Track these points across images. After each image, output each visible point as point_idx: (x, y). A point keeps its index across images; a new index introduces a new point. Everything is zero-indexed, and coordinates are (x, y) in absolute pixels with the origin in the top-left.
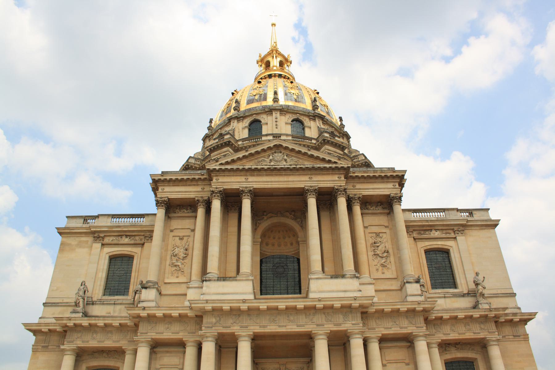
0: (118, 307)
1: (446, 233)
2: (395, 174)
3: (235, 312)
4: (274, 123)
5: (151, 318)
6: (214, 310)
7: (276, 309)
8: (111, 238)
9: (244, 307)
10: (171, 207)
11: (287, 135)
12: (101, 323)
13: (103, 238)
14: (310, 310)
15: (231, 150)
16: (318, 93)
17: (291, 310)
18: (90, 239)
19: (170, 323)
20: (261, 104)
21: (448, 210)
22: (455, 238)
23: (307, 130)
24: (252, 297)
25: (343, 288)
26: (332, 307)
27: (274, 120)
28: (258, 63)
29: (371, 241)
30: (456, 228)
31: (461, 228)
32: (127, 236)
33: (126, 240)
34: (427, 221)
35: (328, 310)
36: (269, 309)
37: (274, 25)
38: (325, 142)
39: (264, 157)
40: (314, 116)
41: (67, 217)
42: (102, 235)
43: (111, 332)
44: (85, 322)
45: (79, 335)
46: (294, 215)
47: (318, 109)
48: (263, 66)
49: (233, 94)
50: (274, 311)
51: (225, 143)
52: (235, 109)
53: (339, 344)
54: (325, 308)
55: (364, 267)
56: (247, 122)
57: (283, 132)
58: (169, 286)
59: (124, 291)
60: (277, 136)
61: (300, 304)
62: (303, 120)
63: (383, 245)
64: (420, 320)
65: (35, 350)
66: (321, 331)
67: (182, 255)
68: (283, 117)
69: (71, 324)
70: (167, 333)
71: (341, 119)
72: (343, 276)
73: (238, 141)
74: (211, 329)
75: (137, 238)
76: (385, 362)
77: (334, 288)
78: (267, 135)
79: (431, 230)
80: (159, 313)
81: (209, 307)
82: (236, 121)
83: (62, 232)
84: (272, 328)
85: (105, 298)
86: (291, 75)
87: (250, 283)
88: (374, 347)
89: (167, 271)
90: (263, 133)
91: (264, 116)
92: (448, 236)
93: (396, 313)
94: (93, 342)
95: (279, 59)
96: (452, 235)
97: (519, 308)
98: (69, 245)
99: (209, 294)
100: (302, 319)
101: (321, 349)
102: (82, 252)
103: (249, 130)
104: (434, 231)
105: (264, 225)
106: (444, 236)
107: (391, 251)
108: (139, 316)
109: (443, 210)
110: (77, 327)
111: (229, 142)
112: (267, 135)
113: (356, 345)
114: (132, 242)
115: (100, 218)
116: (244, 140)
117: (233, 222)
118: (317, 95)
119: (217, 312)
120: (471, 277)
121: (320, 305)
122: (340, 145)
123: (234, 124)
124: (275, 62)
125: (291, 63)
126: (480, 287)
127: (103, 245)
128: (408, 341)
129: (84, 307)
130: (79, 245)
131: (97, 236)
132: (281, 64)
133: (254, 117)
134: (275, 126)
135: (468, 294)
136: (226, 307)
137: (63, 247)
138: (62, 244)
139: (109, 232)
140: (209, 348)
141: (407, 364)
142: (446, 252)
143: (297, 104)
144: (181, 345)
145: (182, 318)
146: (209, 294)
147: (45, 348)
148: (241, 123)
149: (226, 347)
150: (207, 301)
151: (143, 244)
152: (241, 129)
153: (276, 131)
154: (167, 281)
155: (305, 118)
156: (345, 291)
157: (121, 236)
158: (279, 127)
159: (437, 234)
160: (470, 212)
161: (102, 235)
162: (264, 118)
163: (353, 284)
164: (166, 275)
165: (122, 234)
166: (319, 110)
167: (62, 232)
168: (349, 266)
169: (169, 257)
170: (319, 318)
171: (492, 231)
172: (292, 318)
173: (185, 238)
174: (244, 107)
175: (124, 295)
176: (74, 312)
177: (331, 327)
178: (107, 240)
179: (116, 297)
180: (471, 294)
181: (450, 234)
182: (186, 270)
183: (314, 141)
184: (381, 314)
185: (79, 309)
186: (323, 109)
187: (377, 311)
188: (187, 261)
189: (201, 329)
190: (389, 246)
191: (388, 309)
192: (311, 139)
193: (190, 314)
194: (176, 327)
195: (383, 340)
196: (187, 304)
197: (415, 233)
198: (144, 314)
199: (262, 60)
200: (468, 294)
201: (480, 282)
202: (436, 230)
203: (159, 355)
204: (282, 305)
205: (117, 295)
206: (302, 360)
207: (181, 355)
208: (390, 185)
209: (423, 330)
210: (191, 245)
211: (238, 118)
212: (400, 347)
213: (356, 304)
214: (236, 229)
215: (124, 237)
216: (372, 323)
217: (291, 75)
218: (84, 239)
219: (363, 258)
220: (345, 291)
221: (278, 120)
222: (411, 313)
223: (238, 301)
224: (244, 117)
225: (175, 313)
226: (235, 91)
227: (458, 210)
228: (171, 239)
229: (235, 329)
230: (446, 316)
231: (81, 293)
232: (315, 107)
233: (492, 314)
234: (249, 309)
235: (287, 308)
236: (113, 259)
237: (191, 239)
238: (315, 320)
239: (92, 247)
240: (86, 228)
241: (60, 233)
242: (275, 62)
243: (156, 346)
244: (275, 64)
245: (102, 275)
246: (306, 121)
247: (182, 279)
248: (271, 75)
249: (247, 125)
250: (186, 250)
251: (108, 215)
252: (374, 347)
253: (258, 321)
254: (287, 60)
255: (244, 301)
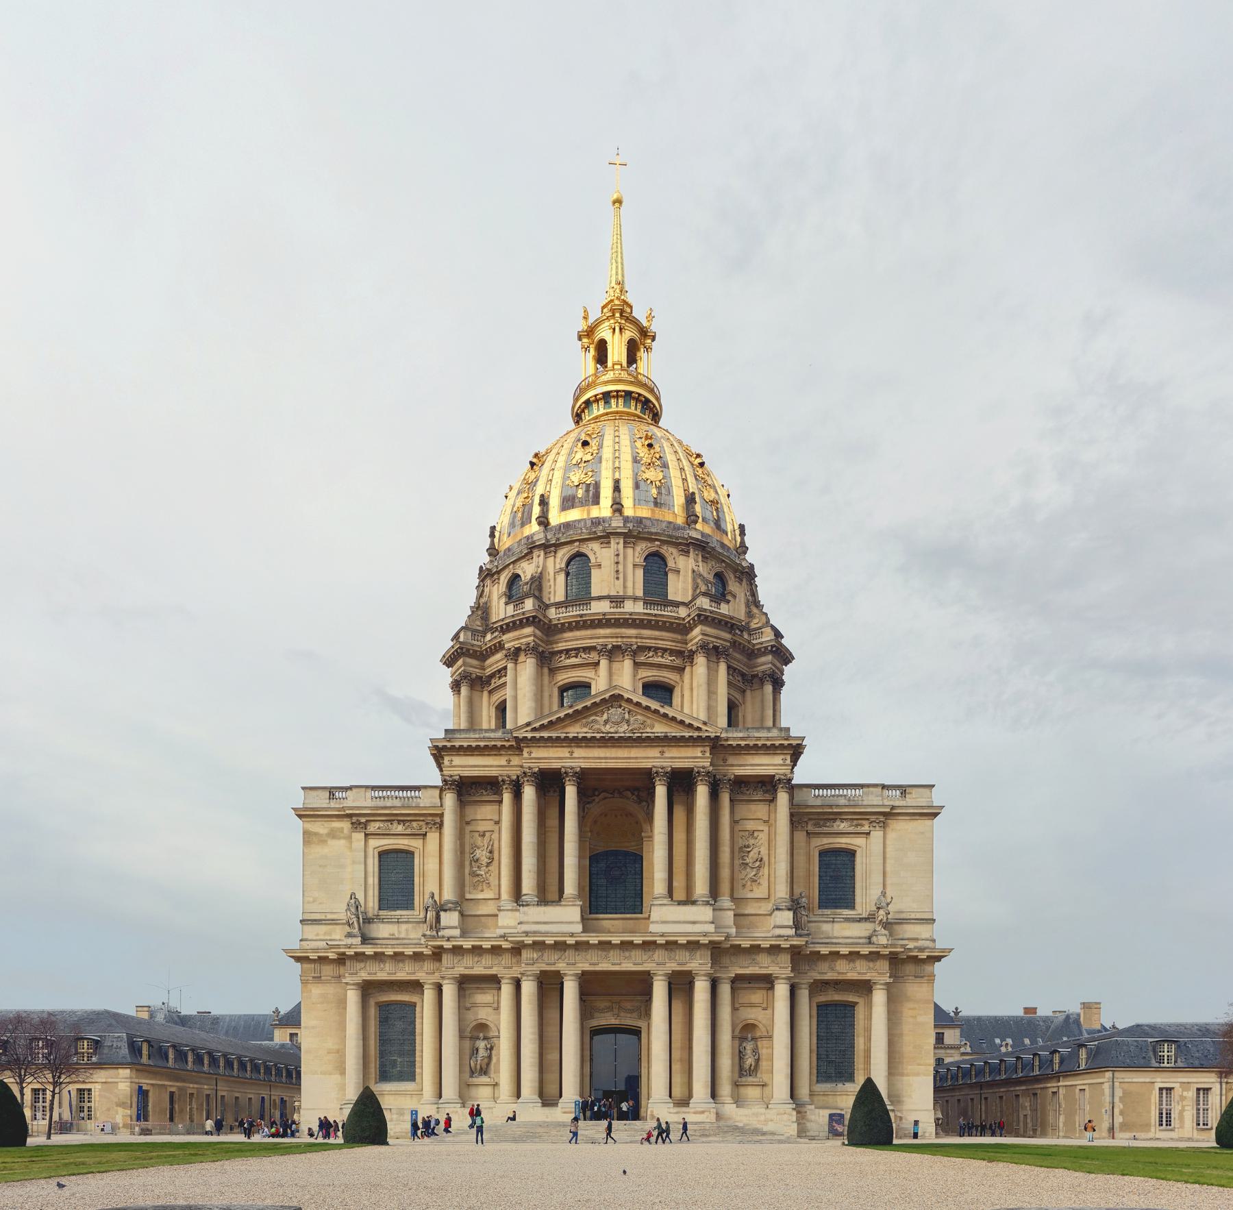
0: (404, 927)
1: (857, 825)
2: (786, 743)
3: (560, 946)
4: (613, 567)
5: (457, 950)
6: (535, 943)
7: (609, 943)
8: (377, 825)
9: (571, 941)
10: (468, 790)
11: (635, 599)
12: (389, 951)
13: (366, 825)
14: (648, 946)
15: (538, 632)
16: (702, 465)
17: (626, 946)
18: (345, 825)
19: (480, 955)
20: (589, 513)
21: (868, 786)
22: (868, 834)
23: (670, 576)
24: (578, 928)
25: (692, 919)
26: (676, 942)
27: (614, 559)
28: (580, 339)
29: (741, 843)
30: (873, 818)
31: (882, 818)
32: (399, 822)
33: (400, 829)
34: (831, 806)
35: (671, 946)
36: (600, 943)
37: (618, 202)
38: (702, 618)
39: (595, 714)
40: (688, 545)
41: (303, 788)
42: (363, 820)
43: (403, 961)
44: (369, 950)
45: (362, 965)
46: (638, 796)
47: (696, 522)
48: (592, 351)
49: (532, 464)
50: (605, 946)
51: (527, 619)
52: (540, 524)
53: (681, 985)
54: (668, 943)
55: (725, 887)
56: (564, 554)
57: (630, 593)
58: (471, 904)
59: (408, 904)
60: (617, 600)
61: (638, 940)
62: (667, 555)
63: (756, 850)
64: (785, 959)
65: (304, 982)
66: (660, 967)
67: (485, 861)
68: (630, 551)
69: (350, 952)
70: (480, 967)
71: (742, 527)
72: (694, 903)
73: (548, 606)
74: (531, 965)
75: (415, 824)
76: (737, 1005)
77: (682, 918)
78: (600, 598)
79: (835, 820)
80: (467, 944)
81: (529, 940)
82: (542, 553)
83: (302, 814)
84: (604, 966)
85: (381, 913)
86: (651, 391)
87: (578, 909)
88: (725, 990)
89: (467, 882)
90: (595, 592)
91: (595, 546)
92: (859, 829)
93: (756, 949)
94: (383, 973)
95: (628, 335)
96: (866, 828)
97: (934, 941)
98: (316, 834)
99: (527, 923)
100: (637, 955)
101: (659, 990)
102: (338, 845)
103: (567, 574)
104: (838, 823)
105: (595, 809)
106: (851, 829)
107: (766, 859)
108: (441, 947)
109: (862, 786)
110: (360, 957)
111: (534, 617)
112: (600, 598)
113: (701, 990)
114: (409, 831)
115: (354, 790)
116: (558, 605)
117: (553, 812)
118: (700, 471)
119: (539, 946)
120: (875, 892)
121: (661, 941)
122: (727, 623)
123: (539, 557)
124: (617, 352)
125: (653, 340)
126: (882, 912)
127: (366, 835)
128: (767, 982)
129: (360, 929)
130: (333, 834)
131: (359, 821)
132: (633, 350)
133: (574, 549)
134: (613, 574)
135: (866, 919)
136: (550, 941)
137: (308, 837)
138: (306, 833)
139: (373, 817)
140: (529, 988)
141: (765, 1009)
142: (851, 854)
143: (660, 514)
144: (494, 981)
145: (496, 950)
146: (527, 923)
147: (318, 979)
148: (550, 560)
149: (550, 985)
150: (527, 934)
151: (425, 835)
152: (552, 574)
153: (616, 589)
154: (468, 896)
155: (671, 549)
156: (694, 923)
157: (391, 821)
158: (621, 576)
159: (843, 826)
160: (904, 790)
161: (363, 820)
162: (596, 552)
163: (705, 913)
164: (467, 889)
165: (392, 818)
166: (699, 526)
167: (302, 814)
168: (701, 887)
169: (467, 863)
170: (659, 955)
171: (928, 822)
172: (627, 954)
173: (488, 834)
174: (556, 517)
175: (407, 909)
176: (349, 935)
177: (672, 966)
178: (373, 827)
179: (399, 912)
180: (870, 918)
181: (862, 825)
182: (493, 881)
183: (683, 612)
184: (737, 950)
185: (356, 931)
186: (708, 515)
187: (732, 946)
188: (493, 868)
189: (519, 962)
190: (764, 851)
191: (746, 944)
192: (677, 604)
193: (506, 945)
194: (487, 960)
195: (737, 981)
196: (500, 932)
197: (810, 823)
198: (447, 945)
199: (590, 332)
200: (866, 919)
201: (884, 904)
202: (842, 820)
203: (467, 992)
204: (616, 940)
205: (398, 908)
206: (639, 998)
207: (495, 992)
208: (778, 760)
209: (788, 972)
210: (496, 846)
211: (549, 548)
212: (760, 988)
213: (704, 940)
214: (556, 822)
215: (395, 824)
216: (726, 960)
217: (651, 391)
218: (337, 824)
219: (725, 873)
220: (694, 923)
221: (621, 558)
222: (774, 950)
223: (564, 934)
224: (558, 546)
225: (487, 945)
226: (536, 455)
227: (884, 787)
228: (467, 836)
229: (561, 966)
230: (824, 950)
231: (353, 910)
232: (691, 518)
233: (886, 951)
234: (577, 943)
235: (622, 943)
236: (383, 855)
237: (495, 836)
238: (656, 956)
239: (349, 838)
240: (339, 809)
241: (300, 816)
242: (617, 352)
243: (465, 983)
244: (616, 359)
245: (373, 880)
246: (671, 553)
247: (488, 894)
248: (609, 392)
249: (563, 565)
250: (491, 852)
251: (367, 787)
252: (725, 990)
253: (589, 957)
254: (644, 332)
255: (572, 935)
